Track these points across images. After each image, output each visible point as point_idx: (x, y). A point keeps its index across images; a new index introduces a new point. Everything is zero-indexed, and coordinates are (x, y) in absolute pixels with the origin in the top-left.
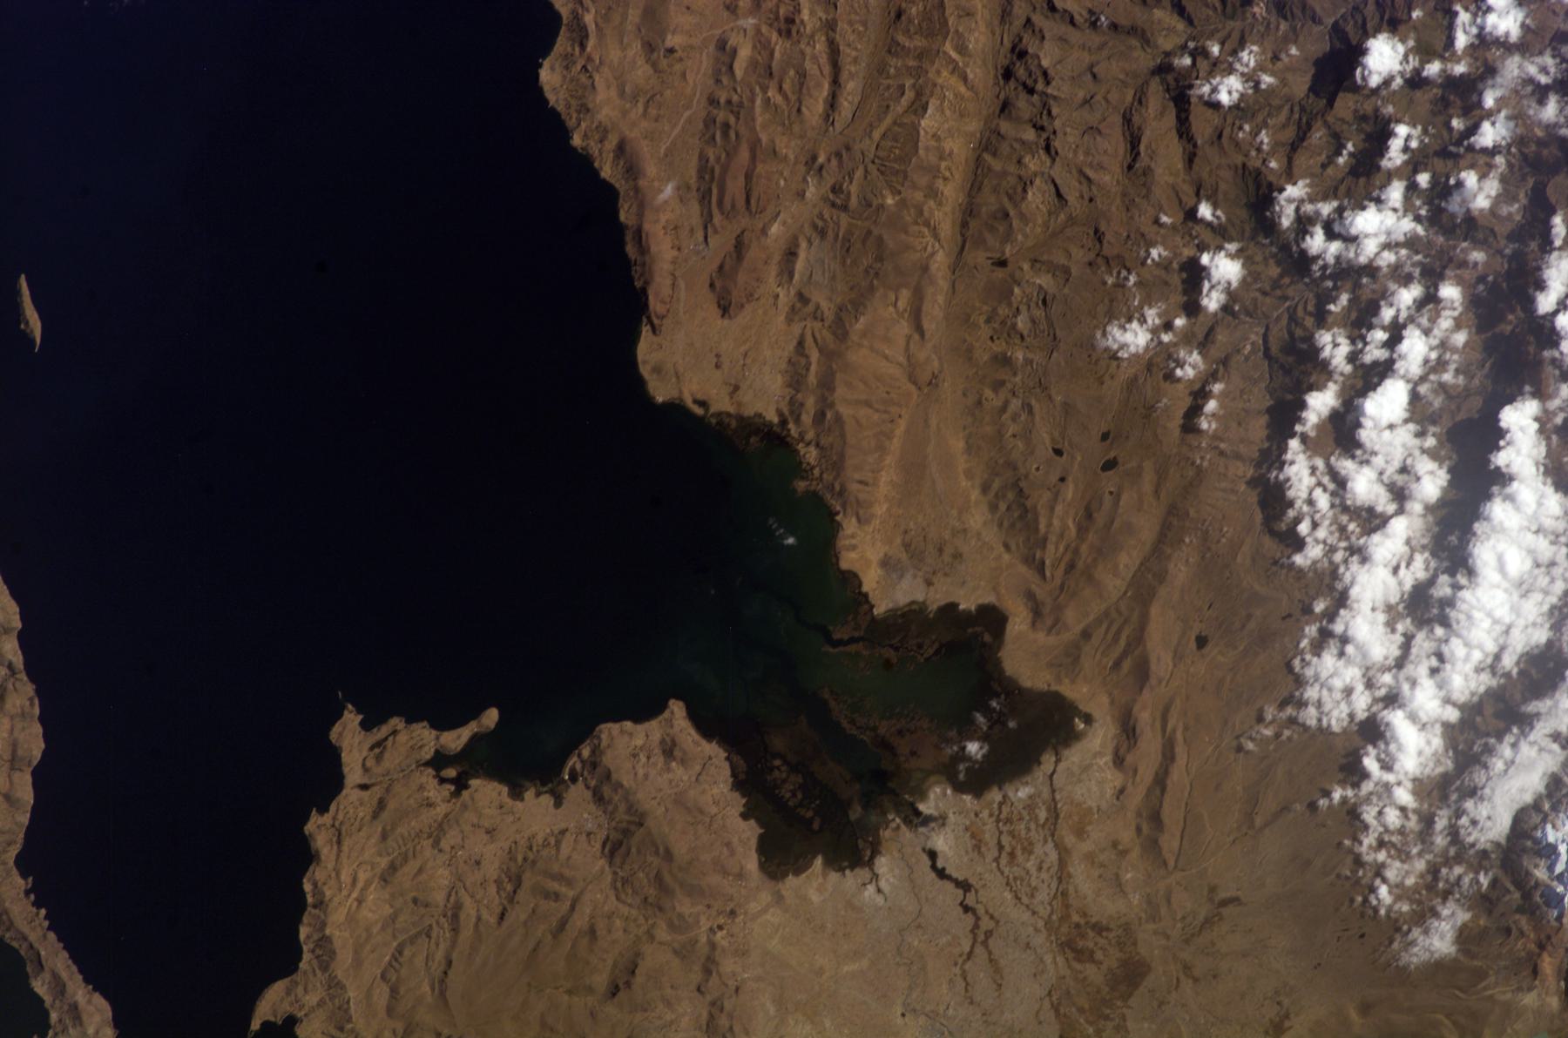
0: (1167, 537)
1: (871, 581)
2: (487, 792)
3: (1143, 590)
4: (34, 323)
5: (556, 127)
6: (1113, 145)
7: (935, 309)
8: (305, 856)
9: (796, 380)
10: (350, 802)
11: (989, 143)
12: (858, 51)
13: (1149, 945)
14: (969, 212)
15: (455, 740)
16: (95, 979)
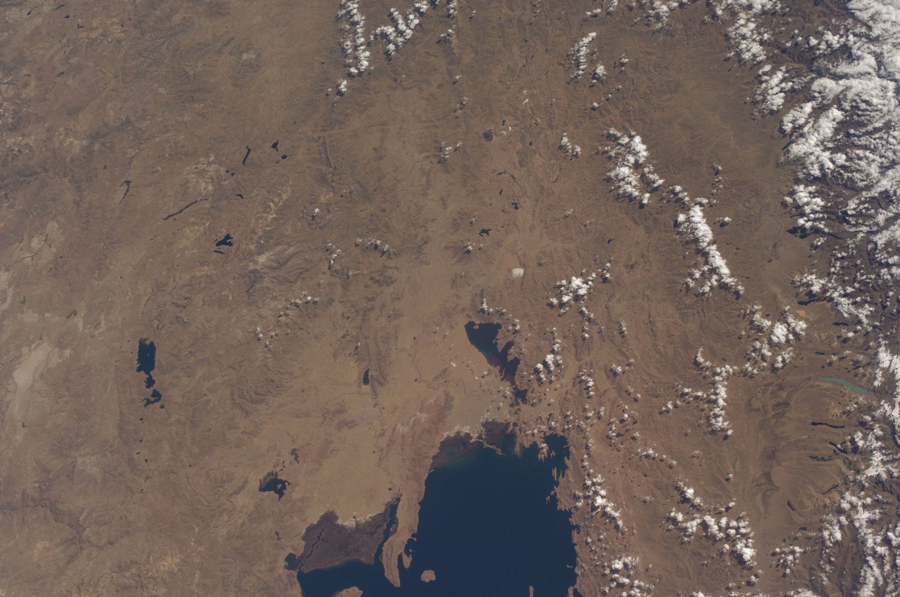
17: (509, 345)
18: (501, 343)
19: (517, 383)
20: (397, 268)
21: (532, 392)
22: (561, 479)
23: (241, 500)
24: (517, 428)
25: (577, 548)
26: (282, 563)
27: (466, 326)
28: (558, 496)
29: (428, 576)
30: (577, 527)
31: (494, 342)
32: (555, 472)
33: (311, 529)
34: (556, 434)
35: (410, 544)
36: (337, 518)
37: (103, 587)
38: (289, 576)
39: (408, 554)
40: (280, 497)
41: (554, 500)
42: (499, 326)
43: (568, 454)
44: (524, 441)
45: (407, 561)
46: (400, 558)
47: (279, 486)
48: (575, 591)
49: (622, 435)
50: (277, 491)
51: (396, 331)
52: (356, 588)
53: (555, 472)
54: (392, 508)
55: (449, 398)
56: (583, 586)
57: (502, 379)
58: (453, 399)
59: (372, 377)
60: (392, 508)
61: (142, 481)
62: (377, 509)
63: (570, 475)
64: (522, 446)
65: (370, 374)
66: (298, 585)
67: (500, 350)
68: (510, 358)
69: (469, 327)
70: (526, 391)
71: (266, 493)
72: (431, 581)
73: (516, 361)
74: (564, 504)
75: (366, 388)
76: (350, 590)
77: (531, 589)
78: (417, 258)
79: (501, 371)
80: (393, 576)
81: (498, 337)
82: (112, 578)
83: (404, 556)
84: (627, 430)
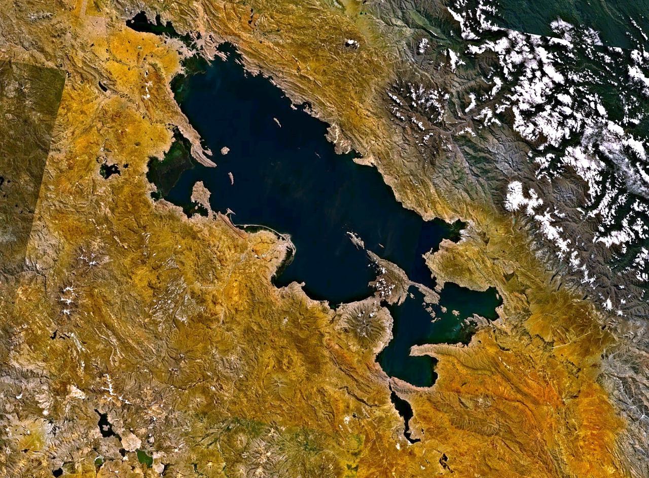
0: (466, 206)
1: (450, 223)
2: (435, 253)
3: (467, 210)
4: (382, 246)
5: (406, 209)
6: (444, 184)
7: (440, 202)
8: (427, 266)
9: (435, 214)
10: (427, 260)
11: (436, 190)
12: (423, 190)
13: (484, 231)
14: (438, 195)
15: (431, 251)
16: (420, 283)
17: (158, 18)
18: (152, 18)
19: (179, 33)
20: (59, 22)
21: (191, 33)
22: (243, 62)
23: (100, 191)
24: (201, 55)
25: (278, 86)
26: (151, 200)
27: (127, 25)
28: (249, 71)
29: (225, 151)
30: (270, 77)
31: (149, 22)
32: (237, 61)
33: (148, 175)
34: (222, 44)
35: (203, 145)
36: (156, 159)
37: (74, 281)
38: (161, 202)
39: (206, 149)
40: (119, 174)
41: (249, 74)
42: (143, 13)
43: (235, 48)
44: (210, 56)
45: (209, 152)
46: (204, 153)
47: (113, 169)
48: (294, 105)
49: (252, 21)
50: (115, 172)
51: (94, 54)
52: (198, 182)
53: (237, 61)
54: (178, 135)
55: (154, 66)
56: (296, 100)
57: (171, 38)
58: (156, 65)
59: (104, 84)
60: (178, 135)
61: (39, 222)
62: (170, 139)
63: (245, 57)
64: (211, 61)
65: (102, 84)
66: (169, 203)
67: (156, 24)
68: (165, 24)
69: (128, 23)
70: (188, 34)
71: (110, 178)
72: (228, 152)
73: (169, 24)
74: (255, 72)
75: (108, 92)
76: (195, 185)
77: (275, 119)
78: (65, 9)
79: (166, 34)
80: (209, 163)
81: (148, 19)
82: (73, 274)
83: (206, 151)
84: (252, 17)
